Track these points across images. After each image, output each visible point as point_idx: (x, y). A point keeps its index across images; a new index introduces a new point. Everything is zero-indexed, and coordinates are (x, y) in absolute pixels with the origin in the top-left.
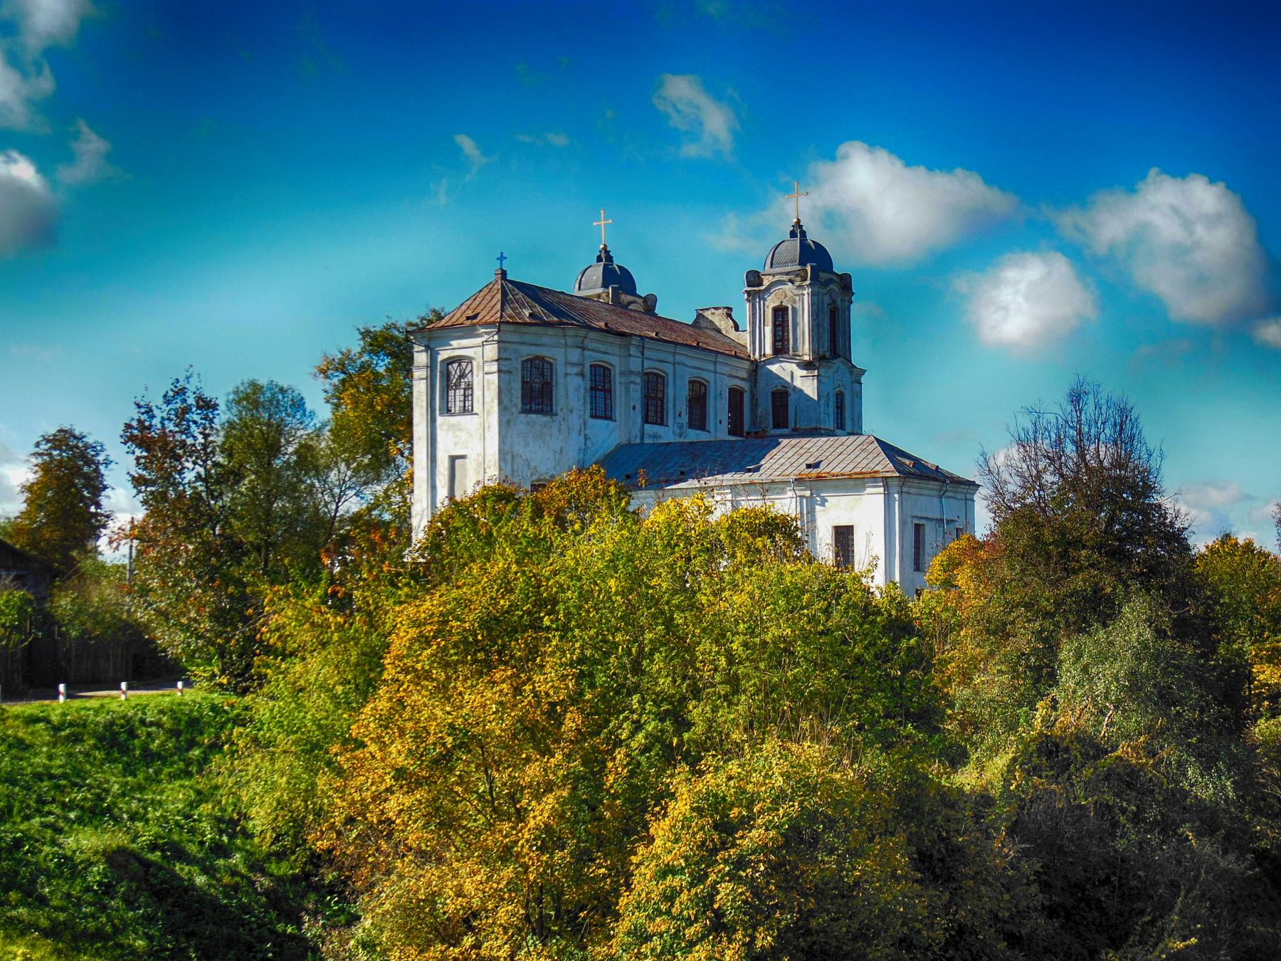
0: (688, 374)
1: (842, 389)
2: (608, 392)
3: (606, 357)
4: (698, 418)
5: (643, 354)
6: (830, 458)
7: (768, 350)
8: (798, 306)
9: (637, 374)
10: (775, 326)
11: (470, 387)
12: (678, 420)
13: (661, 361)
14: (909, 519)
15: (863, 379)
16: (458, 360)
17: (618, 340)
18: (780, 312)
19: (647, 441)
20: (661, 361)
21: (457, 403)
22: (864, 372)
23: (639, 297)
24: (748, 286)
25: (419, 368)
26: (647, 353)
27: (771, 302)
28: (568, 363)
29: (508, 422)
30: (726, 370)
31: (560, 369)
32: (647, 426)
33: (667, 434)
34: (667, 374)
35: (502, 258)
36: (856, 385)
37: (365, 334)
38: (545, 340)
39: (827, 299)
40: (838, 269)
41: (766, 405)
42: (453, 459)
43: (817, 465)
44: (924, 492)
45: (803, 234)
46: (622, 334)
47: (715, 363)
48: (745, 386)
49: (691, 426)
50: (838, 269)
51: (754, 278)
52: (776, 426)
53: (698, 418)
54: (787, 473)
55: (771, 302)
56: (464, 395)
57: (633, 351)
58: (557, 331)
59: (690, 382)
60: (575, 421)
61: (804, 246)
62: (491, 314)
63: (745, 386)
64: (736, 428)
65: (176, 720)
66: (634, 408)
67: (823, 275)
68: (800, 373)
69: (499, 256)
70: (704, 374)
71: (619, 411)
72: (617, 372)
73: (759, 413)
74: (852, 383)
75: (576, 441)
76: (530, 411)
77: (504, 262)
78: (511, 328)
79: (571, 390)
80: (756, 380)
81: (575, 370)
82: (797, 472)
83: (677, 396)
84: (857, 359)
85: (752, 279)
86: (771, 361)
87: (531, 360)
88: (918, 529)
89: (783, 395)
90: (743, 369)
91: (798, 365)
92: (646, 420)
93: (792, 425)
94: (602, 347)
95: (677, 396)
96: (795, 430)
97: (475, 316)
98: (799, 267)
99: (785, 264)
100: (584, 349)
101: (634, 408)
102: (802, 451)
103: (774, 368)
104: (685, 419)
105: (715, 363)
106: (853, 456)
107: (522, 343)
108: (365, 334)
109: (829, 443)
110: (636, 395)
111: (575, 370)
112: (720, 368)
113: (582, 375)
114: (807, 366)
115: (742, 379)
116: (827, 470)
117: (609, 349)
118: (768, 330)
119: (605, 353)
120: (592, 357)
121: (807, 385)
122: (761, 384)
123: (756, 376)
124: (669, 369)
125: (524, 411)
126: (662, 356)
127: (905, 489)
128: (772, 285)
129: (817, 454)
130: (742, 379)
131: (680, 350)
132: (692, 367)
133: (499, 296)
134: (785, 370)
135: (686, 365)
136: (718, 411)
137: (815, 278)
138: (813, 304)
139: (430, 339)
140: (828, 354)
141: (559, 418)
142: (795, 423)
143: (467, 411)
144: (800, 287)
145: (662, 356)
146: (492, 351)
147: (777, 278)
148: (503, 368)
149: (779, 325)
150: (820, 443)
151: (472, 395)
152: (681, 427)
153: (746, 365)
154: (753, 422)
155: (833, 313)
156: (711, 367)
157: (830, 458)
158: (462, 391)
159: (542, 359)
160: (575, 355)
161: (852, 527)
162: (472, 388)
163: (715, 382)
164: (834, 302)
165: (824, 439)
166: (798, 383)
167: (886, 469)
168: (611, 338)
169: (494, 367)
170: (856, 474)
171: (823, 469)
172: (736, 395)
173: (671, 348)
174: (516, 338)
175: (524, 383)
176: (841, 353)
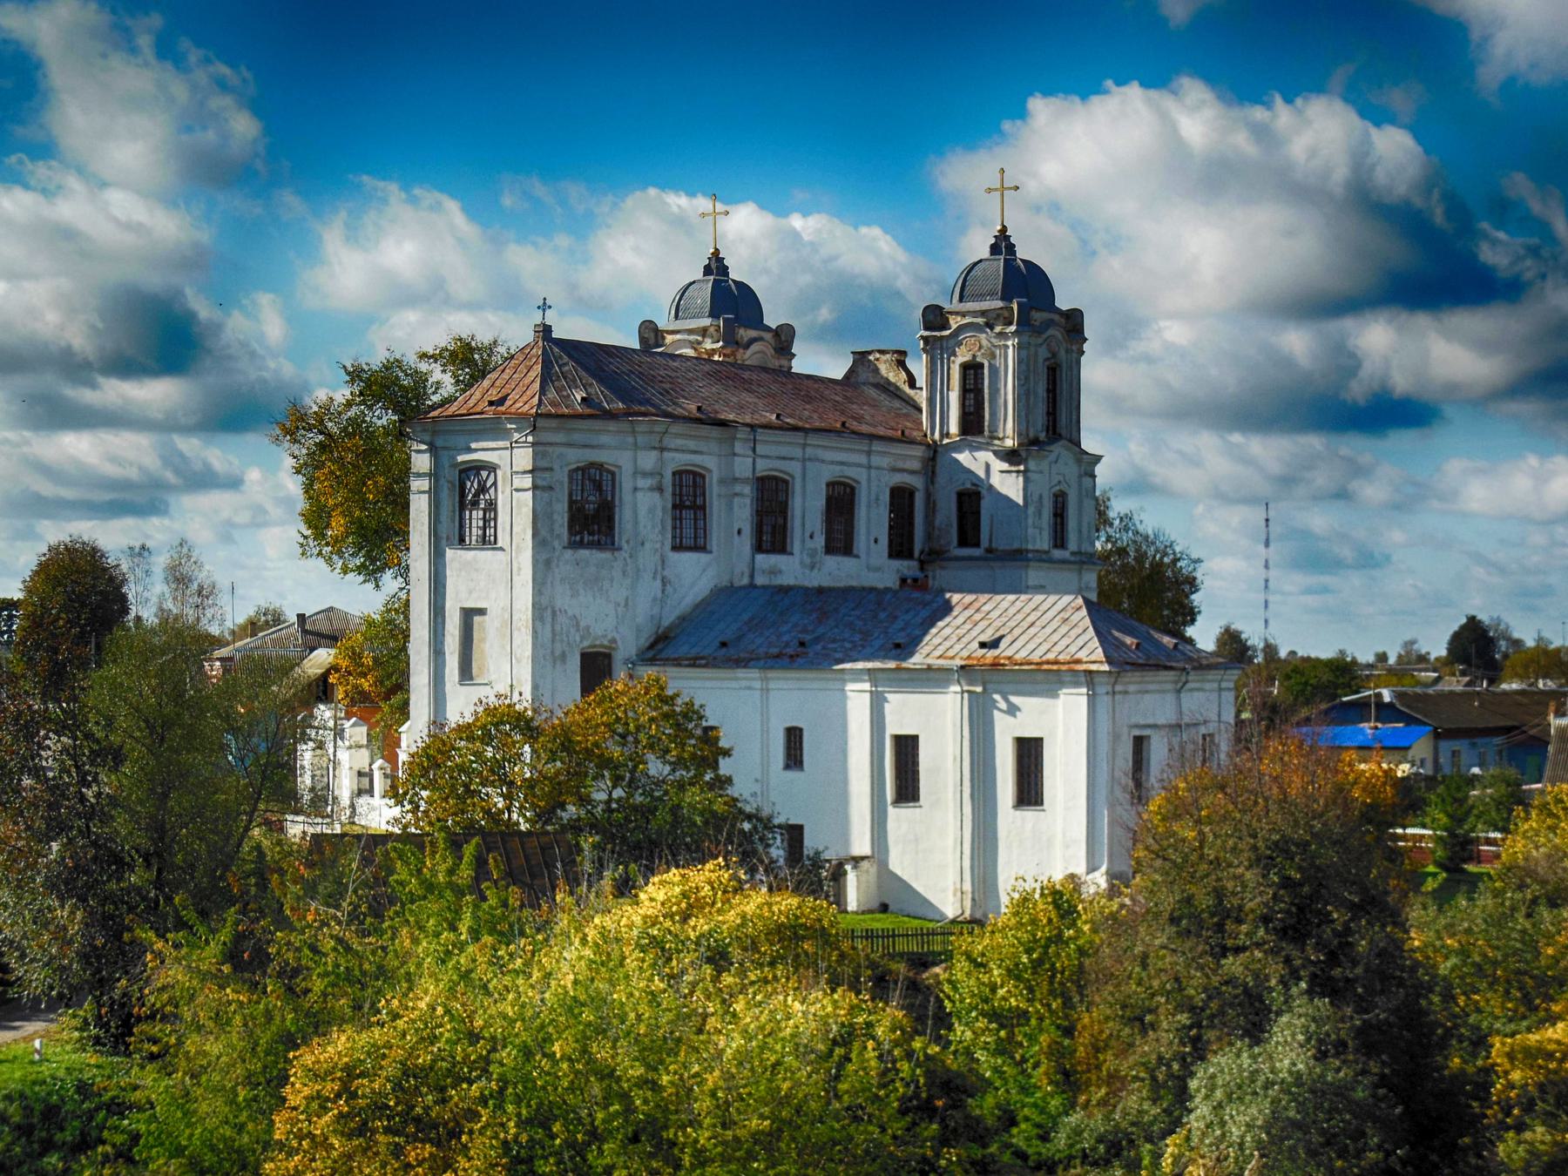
0: (828, 473)
1: (1063, 487)
2: (700, 509)
3: (697, 459)
4: (840, 540)
5: (754, 450)
6: (1017, 632)
7: (954, 428)
8: (999, 362)
9: (745, 481)
10: (965, 391)
11: (492, 506)
12: (810, 544)
13: (784, 458)
14: (1125, 730)
15: (1098, 469)
16: (477, 467)
17: (715, 432)
18: (972, 370)
19: (760, 580)
20: (784, 458)
21: (474, 530)
22: (1098, 459)
23: (768, 329)
24: (926, 329)
25: (419, 475)
26: (760, 449)
27: (963, 356)
28: (637, 473)
29: (548, 563)
30: (885, 462)
31: (626, 482)
32: (760, 557)
33: (790, 569)
34: (793, 477)
35: (544, 307)
36: (1087, 481)
37: (355, 374)
38: (604, 439)
39: (1043, 353)
40: (1063, 302)
41: (947, 511)
42: (469, 615)
43: (994, 644)
44: (1151, 687)
45: (1011, 248)
46: (723, 424)
47: (869, 453)
48: (917, 482)
49: (830, 549)
50: (1063, 302)
51: (935, 317)
52: (963, 542)
53: (840, 540)
54: (951, 653)
55: (963, 356)
56: (484, 519)
57: (739, 447)
58: (624, 426)
59: (828, 485)
60: (648, 558)
61: (1010, 266)
62: (525, 398)
63: (917, 482)
64: (900, 547)
65: (27, 1110)
66: (739, 532)
67: (1038, 317)
68: (998, 465)
70: (851, 472)
71: (716, 537)
72: (715, 480)
73: (937, 523)
74: (1080, 476)
75: (649, 588)
76: (581, 545)
78: (553, 423)
79: (643, 511)
80: (933, 472)
81: (648, 482)
82: (965, 654)
83: (807, 510)
84: (1089, 444)
85: (931, 317)
86: (957, 447)
87: (583, 469)
88: (1139, 743)
89: (972, 497)
90: (913, 457)
91: (995, 453)
92: (759, 548)
93: (985, 543)
94: (692, 444)
95: (807, 510)
96: (989, 550)
97: (502, 401)
98: (1000, 304)
99: (980, 297)
100: (662, 450)
101: (739, 532)
102: (978, 617)
103: (963, 457)
104: (820, 541)
105: (869, 453)
106: (1048, 630)
107: (569, 445)
108: (355, 374)
109: (1019, 604)
110: (743, 513)
111: (648, 482)
112: (876, 460)
113: (660, 489)
114: (1011, 456)
115: (912, 472)
116: (1009, 653)
117: (702, 446)
118: (954, 397)
119: (695, 452)
120: (676, 460)
121: (1008, 484)
122: (941, 479)
123: (934, 467)
124: (794, 468)
125: (574, 545)
126: (784, 451)
127: (1118, 688)
128: (961, 329)
129: (998, 623)
130: (912, 472)
131: (813, 440)
132: (832, 463)
133: (538, 368)
134: (975, 461)
135: (823, 461)
136: (872, 522)
137: (1024, 322)
138: (1020, 362)
139: (435, 433)
140: (1042, 436)
141: (624, 554)
142: (990, 541)
143: (487, 541)
144: (1002, 335)
145: (784, 451)
146: (524, 458)
147: (968, 320)
148: (540, 483)
149: (970, 391)
150: (1005, 604)
151: (495, 519)
152: (813, 553)
153: (918, 452)
154: (929, 536)
155: (1053, 371)
156: (863, 459)
157: (1017, 632)
158: (481, 513)
159: (600, 466)
160: (648, 460)
161: (1041, 739)
162: (495, 510)
163: (869, 480)
164: (1054, 355)
165: (1011, 597)
166: (996, 481)
167: (1093, 658)
168: (705, 430)
169: (527, 482)
170: (1048, 662)
171: (1004, 650)
172: (901, 499)
173: (798, 438)
174: (560, 437)
175: (571, 502)
176: (1064, 432)
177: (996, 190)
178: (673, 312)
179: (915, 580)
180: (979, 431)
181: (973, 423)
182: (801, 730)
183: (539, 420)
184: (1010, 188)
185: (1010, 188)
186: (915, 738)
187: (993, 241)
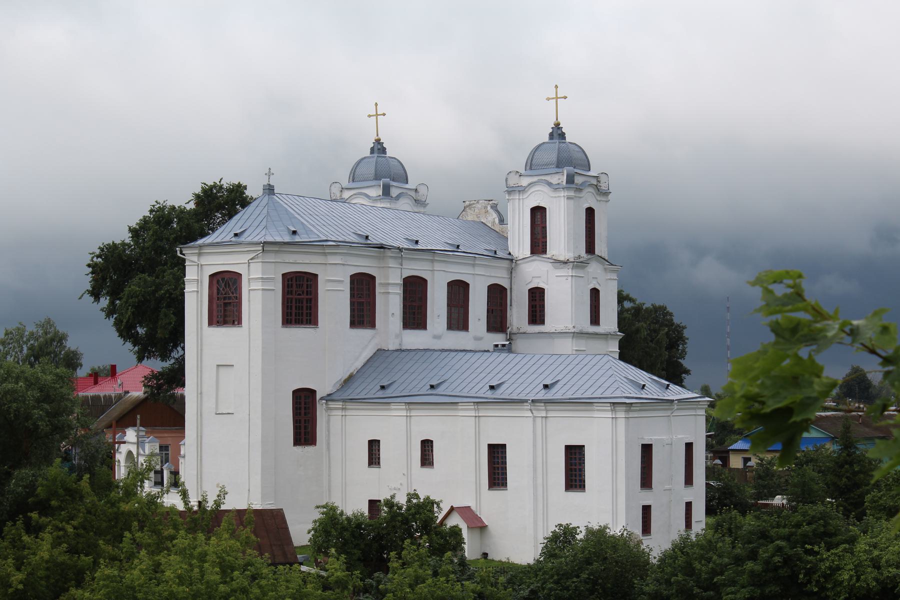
1: (597, 287)
18: (538, 214)
35: (269, 174)
45: (562, 136)
46: (381, 247)
69: (267, 171)
77: (272, 177)
177: (553, 98)
178: (351, 177)
179: (504, 345)
180: (544, 251)
181: (539, 245)
182: (432, 442)
183: (266, 245)
184: (562, 98)
185: (562, 98)
186: (503, 446)
187: (551, 130)
